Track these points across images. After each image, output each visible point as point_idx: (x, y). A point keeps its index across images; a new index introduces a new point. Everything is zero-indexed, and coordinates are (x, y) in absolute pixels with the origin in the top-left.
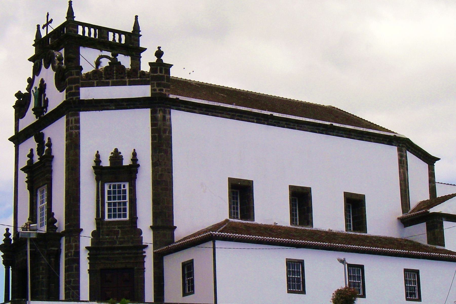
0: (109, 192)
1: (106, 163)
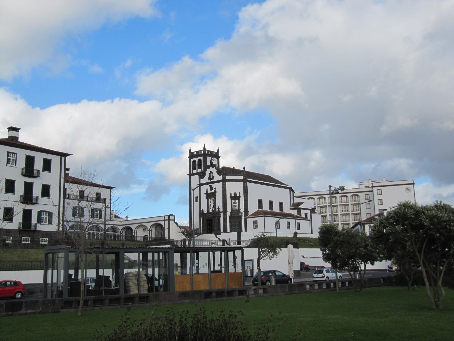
1: (233, 195)
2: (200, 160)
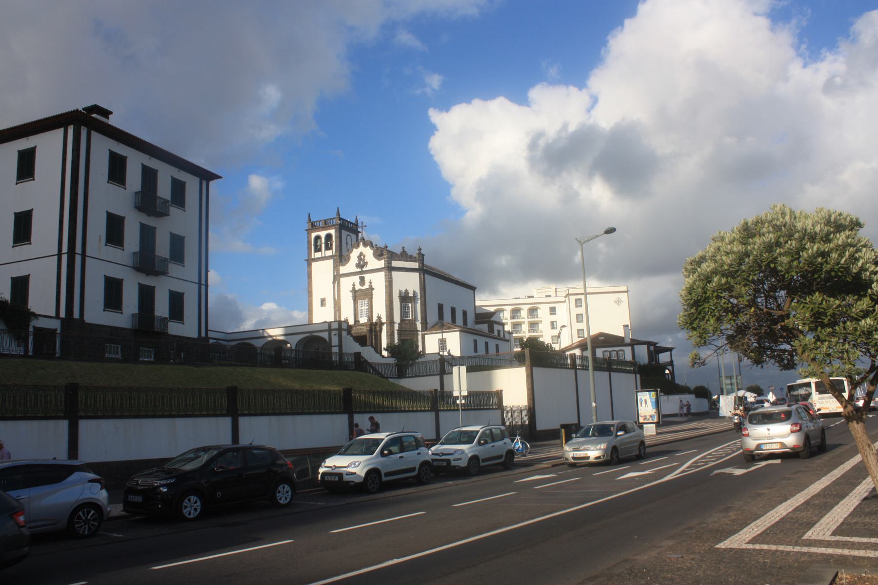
2: (329, 237)
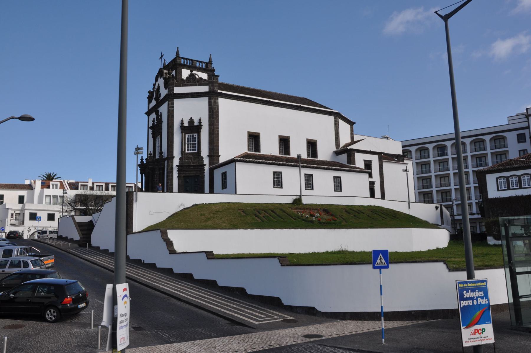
0: (188, 138)
1: (186, 124)
